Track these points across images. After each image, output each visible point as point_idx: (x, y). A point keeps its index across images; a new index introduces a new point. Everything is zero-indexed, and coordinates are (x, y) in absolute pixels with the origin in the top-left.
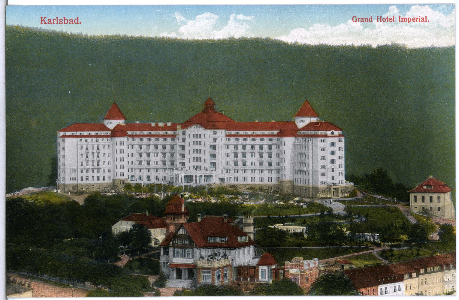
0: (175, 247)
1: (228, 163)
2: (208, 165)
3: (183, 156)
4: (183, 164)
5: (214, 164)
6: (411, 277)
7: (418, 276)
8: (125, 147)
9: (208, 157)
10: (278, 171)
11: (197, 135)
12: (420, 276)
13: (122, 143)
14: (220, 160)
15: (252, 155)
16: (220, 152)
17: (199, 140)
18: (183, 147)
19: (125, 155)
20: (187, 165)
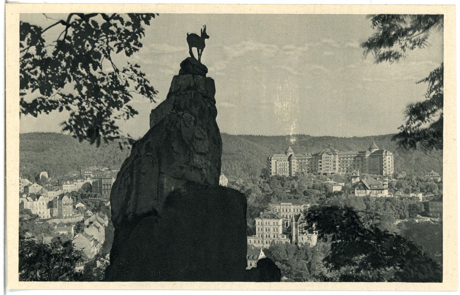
1: (340, 169)
5: (335, 169)
9: (332, 165)
11: (327, 157)
13: (294, 162)
14: (337, 167)
16: (337, 163)
17: (328, 159)
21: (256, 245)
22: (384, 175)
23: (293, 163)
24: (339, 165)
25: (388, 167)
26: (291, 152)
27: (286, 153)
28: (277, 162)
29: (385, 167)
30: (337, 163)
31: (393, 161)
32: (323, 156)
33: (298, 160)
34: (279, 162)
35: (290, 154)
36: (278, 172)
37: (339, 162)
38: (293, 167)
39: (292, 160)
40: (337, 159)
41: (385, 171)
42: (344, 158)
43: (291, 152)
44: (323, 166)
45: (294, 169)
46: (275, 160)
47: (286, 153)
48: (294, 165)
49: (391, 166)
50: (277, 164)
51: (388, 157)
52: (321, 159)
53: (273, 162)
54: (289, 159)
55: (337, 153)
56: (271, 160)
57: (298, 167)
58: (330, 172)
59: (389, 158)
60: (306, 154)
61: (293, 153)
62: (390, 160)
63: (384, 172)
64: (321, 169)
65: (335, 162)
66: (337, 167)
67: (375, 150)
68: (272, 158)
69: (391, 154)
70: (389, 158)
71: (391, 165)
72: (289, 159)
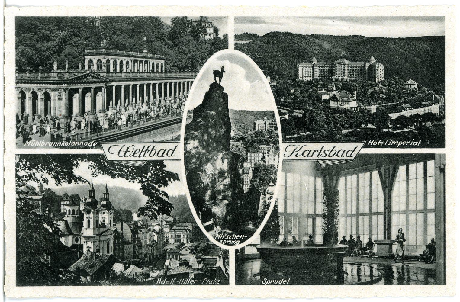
0: (332, 101)
1: (348, 75)
2: (342, 75)
3: (334, 73)
4: (334, 75)
5: (344, 75)
6: (404, 111)
7: (406, 110)
8: (317, 70)
10: (364, 77)
12: (407, 111)
13: (316, 69)
14: (346, 74)
15: (356, 72)
16: (346, 71)
18: (334, 70)
19: (317, 72)
20: (336, 75)
21: (248, 166)
22: (377, 82)
23: (315, 70)
24: (348, 72)
25: (379, 76)
26: (315, 61)
27: (311, 62)
28: (303, 69)
29: (378, 76)
30: (346, 71)
31: (384, 71)
32: (336, 65)
33: (319, 67)
34: (305, 69)
35: (313, 63)
36: (303, 76)
37: (348, 70)
38: (315, 72)
39: (315, 68)
40: (346, 68)
41: (377, 78)
42: (351, 67)
43: (315, 61)
44: (336, 73)
45: (316, 74)
46: (302, 68)
47: (263, 120)
48: (316, 71)
49: (382, 75)
50: (303, 71)
51: (379, 68)
52: (335, 68)
53: (300, 69)
54: (313, 67)
55: (346, 63)
56: (298, 67)
57: (319, 72)
58: (340, 78)
59: (380, 69)
60: (326, 63)
61: (316, 62)
62: (381, 71)
63: (377, 80)
64: (334, 75)
65: (344, 70)
66: (346, 74)
67: (372, 62)
68: (300, 66)
69: (382, 66)
70: (380, 69)
71: (382, 74)
72: (313, 67)
